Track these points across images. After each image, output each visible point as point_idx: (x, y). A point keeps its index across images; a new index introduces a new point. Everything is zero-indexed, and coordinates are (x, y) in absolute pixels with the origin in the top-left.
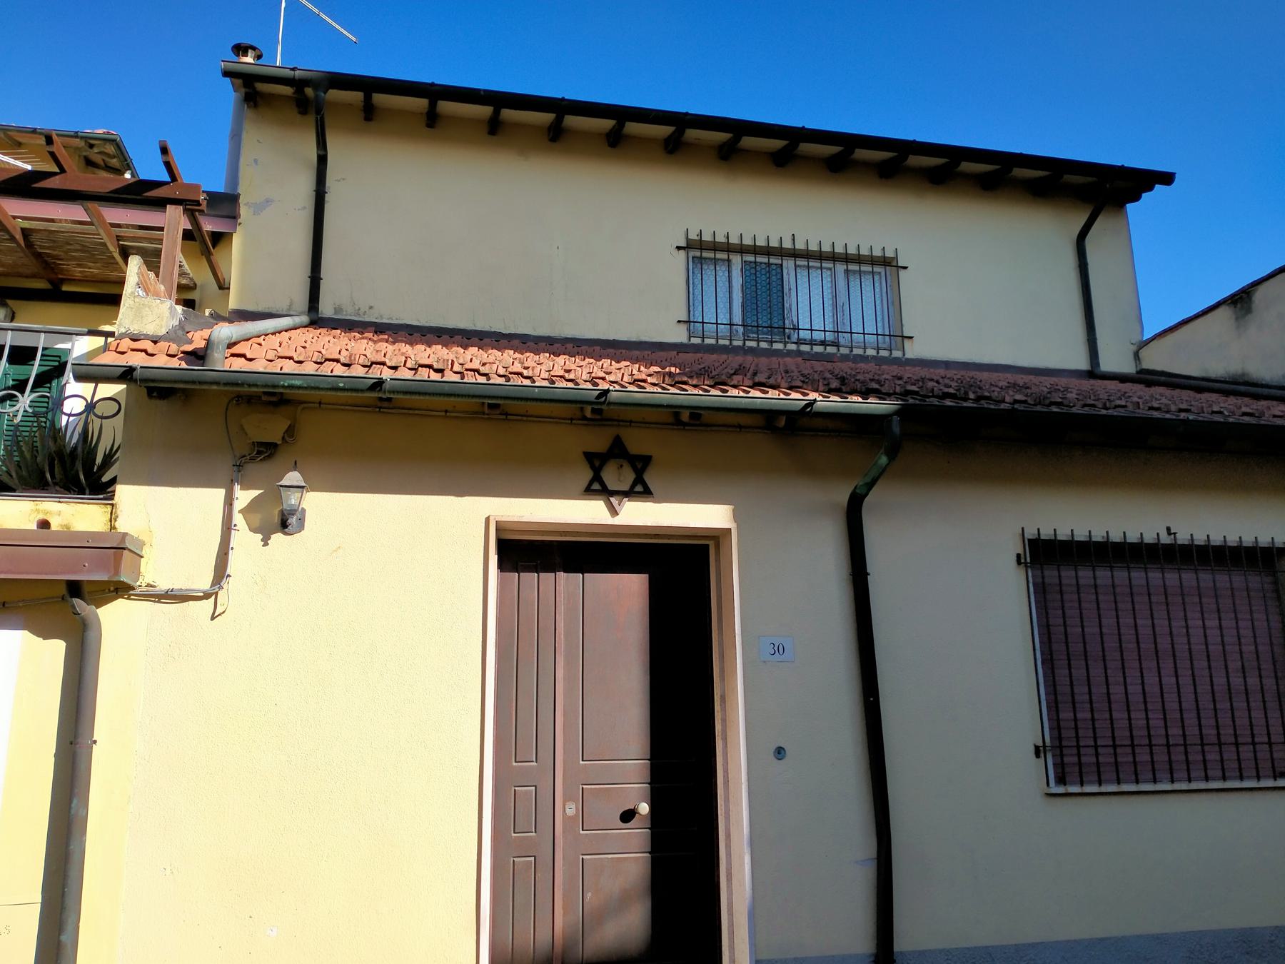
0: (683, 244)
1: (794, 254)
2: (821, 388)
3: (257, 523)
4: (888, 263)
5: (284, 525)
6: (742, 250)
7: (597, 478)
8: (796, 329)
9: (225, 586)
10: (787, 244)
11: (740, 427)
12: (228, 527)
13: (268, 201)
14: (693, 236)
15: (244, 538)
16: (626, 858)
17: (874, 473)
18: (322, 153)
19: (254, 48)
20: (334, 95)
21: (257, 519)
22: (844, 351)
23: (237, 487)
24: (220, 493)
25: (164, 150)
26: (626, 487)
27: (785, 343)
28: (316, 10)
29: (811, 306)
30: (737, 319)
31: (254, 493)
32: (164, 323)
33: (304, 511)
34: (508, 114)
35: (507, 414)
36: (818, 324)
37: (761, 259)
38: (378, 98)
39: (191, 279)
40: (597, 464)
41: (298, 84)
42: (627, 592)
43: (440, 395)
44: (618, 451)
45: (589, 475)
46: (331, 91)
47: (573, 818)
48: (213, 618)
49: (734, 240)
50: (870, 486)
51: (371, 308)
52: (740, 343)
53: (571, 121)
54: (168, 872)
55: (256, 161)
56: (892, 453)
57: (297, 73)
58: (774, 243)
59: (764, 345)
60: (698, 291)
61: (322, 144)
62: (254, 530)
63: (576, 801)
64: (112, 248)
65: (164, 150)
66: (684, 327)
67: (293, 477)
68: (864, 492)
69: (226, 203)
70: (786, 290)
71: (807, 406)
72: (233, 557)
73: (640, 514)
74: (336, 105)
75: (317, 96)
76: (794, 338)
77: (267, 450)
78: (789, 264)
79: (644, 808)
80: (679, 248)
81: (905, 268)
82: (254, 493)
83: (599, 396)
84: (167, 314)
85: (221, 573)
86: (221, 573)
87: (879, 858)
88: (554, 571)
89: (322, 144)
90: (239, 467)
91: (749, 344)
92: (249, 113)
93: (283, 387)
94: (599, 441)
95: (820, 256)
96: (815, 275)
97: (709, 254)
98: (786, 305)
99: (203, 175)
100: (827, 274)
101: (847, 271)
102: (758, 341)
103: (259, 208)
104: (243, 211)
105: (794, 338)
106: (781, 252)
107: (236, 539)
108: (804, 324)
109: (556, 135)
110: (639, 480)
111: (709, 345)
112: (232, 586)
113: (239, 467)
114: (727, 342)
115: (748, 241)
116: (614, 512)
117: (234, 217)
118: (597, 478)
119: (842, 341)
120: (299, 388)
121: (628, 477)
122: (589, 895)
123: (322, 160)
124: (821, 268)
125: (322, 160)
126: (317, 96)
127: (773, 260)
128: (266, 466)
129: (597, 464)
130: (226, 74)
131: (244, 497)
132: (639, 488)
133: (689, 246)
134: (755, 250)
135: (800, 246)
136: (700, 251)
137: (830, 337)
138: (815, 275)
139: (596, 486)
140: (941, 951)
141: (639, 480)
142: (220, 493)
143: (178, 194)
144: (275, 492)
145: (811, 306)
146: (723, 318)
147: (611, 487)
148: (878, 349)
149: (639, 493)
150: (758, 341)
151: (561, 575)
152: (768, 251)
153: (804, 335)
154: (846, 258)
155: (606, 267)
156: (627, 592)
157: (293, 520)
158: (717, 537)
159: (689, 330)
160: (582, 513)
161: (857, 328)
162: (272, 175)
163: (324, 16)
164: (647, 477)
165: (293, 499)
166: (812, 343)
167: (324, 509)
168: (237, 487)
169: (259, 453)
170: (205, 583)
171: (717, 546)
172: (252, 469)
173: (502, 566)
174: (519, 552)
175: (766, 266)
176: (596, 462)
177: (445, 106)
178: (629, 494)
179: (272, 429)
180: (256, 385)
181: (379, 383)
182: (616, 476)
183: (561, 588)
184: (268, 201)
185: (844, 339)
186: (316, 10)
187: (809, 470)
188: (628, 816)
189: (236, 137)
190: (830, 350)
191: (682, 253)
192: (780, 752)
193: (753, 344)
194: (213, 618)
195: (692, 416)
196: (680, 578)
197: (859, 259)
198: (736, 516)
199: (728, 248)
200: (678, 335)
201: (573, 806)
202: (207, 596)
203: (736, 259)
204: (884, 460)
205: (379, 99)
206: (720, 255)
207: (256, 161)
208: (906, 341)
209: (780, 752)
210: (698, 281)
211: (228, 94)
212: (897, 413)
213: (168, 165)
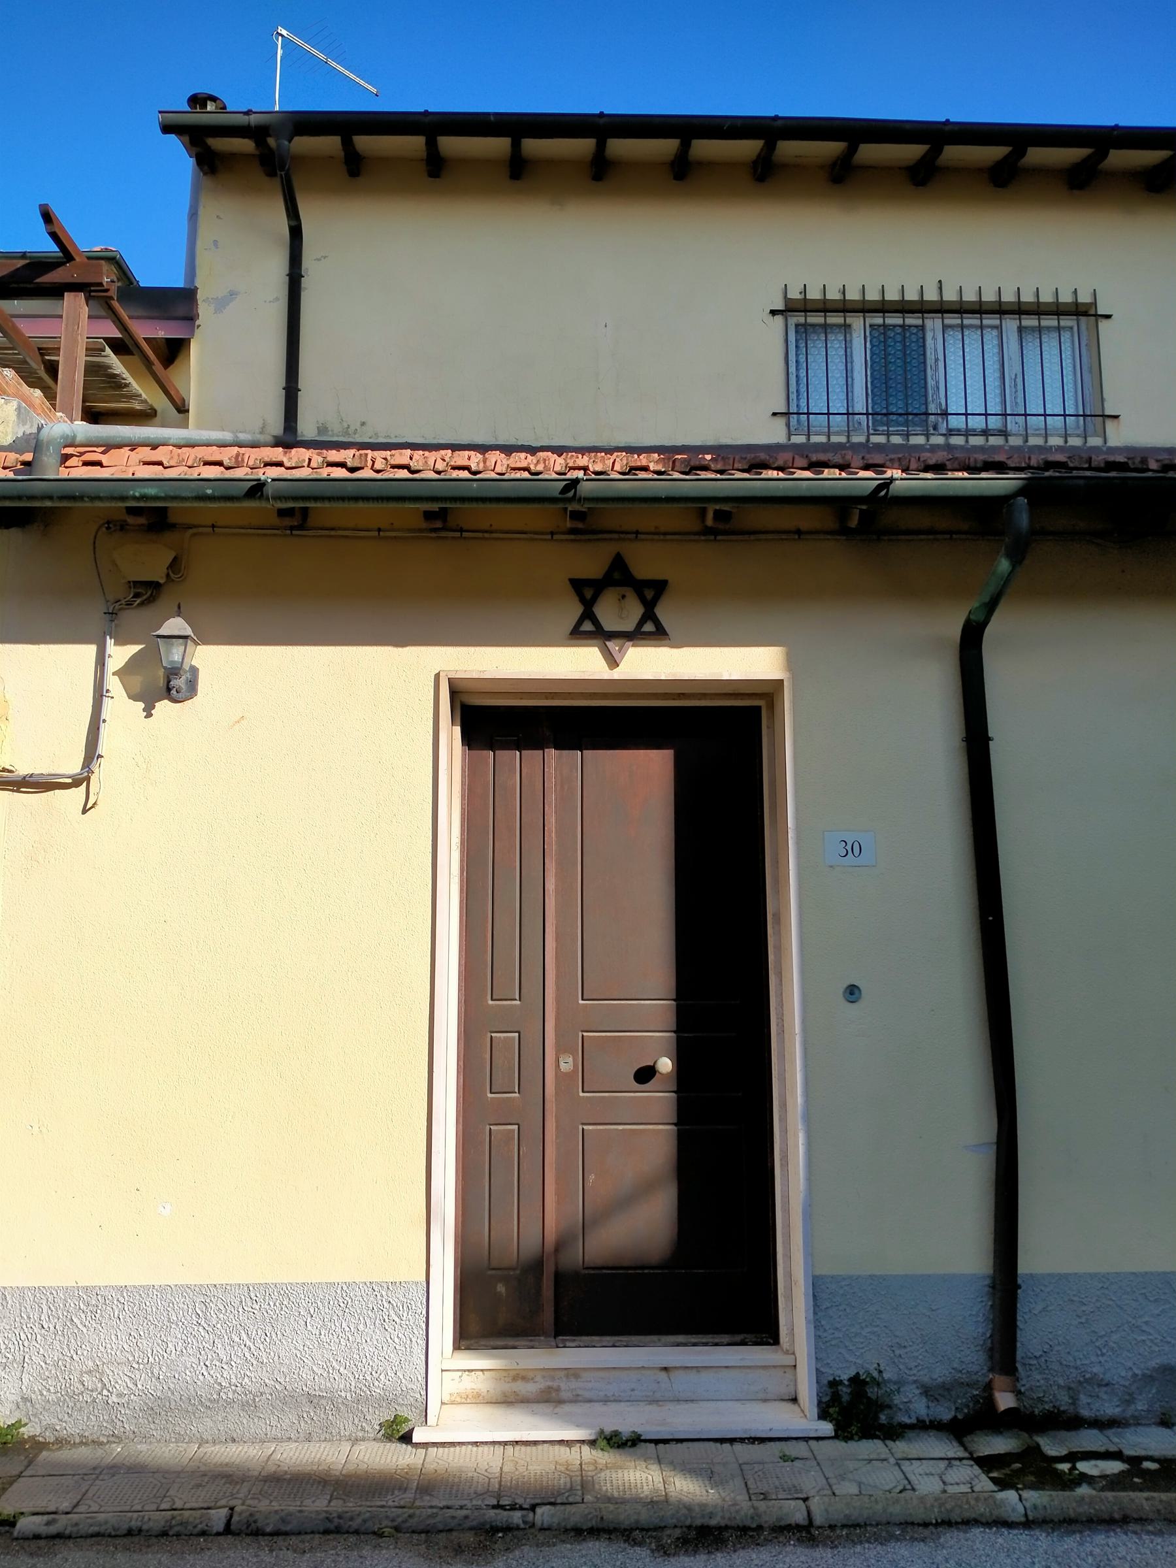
0: (780, 306)
1: (941, 309)
2: (913, 465)
3: (137, 689)
4: (1084, 311)
5: (168, 692)
6: (864, 308)
7: (588, 614)
8: (945, 414)
9: (96, 770)
10: (931, 295)
11: (799, 532)
12: (100, 694)
13: (233, 294)
14: (794, 294)
15: (121, 707)
16: (645, 1132)
17: (992, 589)
18: (293, 223)
19: (214, 99)
20: (304, 144)
21: (137, 681)
22: (1015, 441)
23: (110, 642)
24: (91, 650)
25: (47, 217)
26: (629, 626)
27: (927, 436)
28: (322, 56)
29: (967, 381)
30: (860, 406)
31: (134, 649)
32: (9, 430)
33: (194, 671)
34: (533, 146)
35: (461, 530)
36: (976, 406)
37: (894, 320)
38: (363, 142)
39: (145, 401)
40: (588, 594)
41: (258, 132)
42: (649, 771)
43: (342, 499)
44: (618, 576)
45: (577, 610)
46: (296, 139)
47: (570, 1076)
48: (85, 811)
49: (853, 295)
50: (991, 607)
51: (363, 424)
52: (862, 439)
53: (619, 147)
54: (36, 1129)
55: (216, 243)
56: (1017, 555)
57: (253, 117)
58: (912, 295)
59: (896, 440)
60: (803, 373)
61: (293, 213)
62: (133, 697)
63: (573, 1053)
64: (34, 365)
65: (47, 217)
66: (780, 422)
67: (175, 625)
68: (980, 617)
69: (178, 303)
70: (930, 360)
71: (879, 488)
72: (105, 731)
73: (650, 664)
74: (302, 160)
75: (278, 146)
76: (943, 429)
77: (147, 593)
78: (933, 324)
79: (666, 1065)
80: (773, 313)
81: (1108, 317)
82: (134, 649)
83: (566, 489)
84: (13, 416)
85: (91, 753)
86: (91, 753)
87: (999, 1143)
88: (539, 745)
89: (293, 213)
90: (112, 615)
91: (875, 439)
92: (207, 182)
93: (135, 498)
94: (590, 562)
95: (979, 309)
96: (972, 337)
97: (816, 319)
98: (931, 383)
99: (155, 271)
100: (991, 337)
101: (1021, 329)
102: (888, 435)
103: (220, 305)
104: (204, 310)
105: (943, 429)
106: (922, 308)
107: (108, 706)
108: (955, 406)
109: (601, 174)
110: (649, 615)
111: (817, 445)
112: (103, 772)
113: (112, 615)
114: (843, 439)
115: (873, 296)
116: (613, 663)
117: (190, 318)
118: (588, 614)
119: (1010, 427)
120: (156, 498)
121: (635, 611)
122: (591, 1178)
123: (296, 233)
124: (982, 327)
125: (296, 233)
126: (278, 146)
127: (912, 320)
128: (146, 613)
129: (588, 594)
130: (167, 129)
131: (119, 655)
132: (649, 627)
133: (790, 308)
134: (883, 307)
135: (950, 296)
136: (808, 317)
137: (994, 423)
138: (972, 337)
139: (587, 626)
140: (1093, 1276)
141: (649, 615)
142: (91, 650)
143: (76, 277)
144: (155, 644)
145: (967, 381)
146: (838, 406)
147: (608, 626)
148: (1066, 437)
149: (650, 634)
150: (888, 435)
151: (551, 753)
152: (903, 308)
153: (956, 422)
154: (1019, 310)
155: (657, 343)
156: (646, 776)
157: (179, 682)
158: (769, 692)
159: (788, 425)
160: (572, 664)
161: (1034, 407)
162: (232, 262)
163: (333, 64)
164: (661, 612)
165: (175, 654)
166: (968, 433)
167: (230, 671)
168: (110, 642)
169: (137, 595)
170: (73, 766)
171: (771, 706)
172: (132, 617)
173: (469, 739)
174: (490, 723)
175: (899, 331)
176: (587, 592)
177: (450, 145)
178: (635, 636)
179: (150, 561)
180: (99, 498)
181: (257, 489)
182: (616, 612)
183: (551, 770)
184: (233, 294)
185: (1012, 424)
186: (322, 56)
187: (906, 590)
188: (645, 1074)
189: (193, 216)
190: (994, 441)
191: (779, 319)
192: (852, 992)
193: (881, 439)
194: (85, 811)
195: (720, 516)
196: (718, 756)
197: (1038, 310)
198: (791, 663)
199: (845, 307)
200: (773, 433)
201: (570, 1060)
202: (76, 783)
203: (857, 322)
204: (1004, 565)
205: (364, 143)
206: (835, 319)
207: (216, 243)
208: (1110, 425)
209: (852, 992)
210: (802, 359)
211: (178, 158)
212: (1021, 492)
213: (54, 236)
